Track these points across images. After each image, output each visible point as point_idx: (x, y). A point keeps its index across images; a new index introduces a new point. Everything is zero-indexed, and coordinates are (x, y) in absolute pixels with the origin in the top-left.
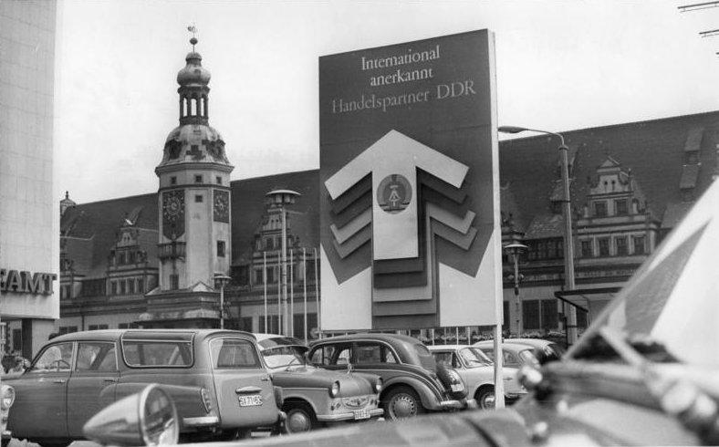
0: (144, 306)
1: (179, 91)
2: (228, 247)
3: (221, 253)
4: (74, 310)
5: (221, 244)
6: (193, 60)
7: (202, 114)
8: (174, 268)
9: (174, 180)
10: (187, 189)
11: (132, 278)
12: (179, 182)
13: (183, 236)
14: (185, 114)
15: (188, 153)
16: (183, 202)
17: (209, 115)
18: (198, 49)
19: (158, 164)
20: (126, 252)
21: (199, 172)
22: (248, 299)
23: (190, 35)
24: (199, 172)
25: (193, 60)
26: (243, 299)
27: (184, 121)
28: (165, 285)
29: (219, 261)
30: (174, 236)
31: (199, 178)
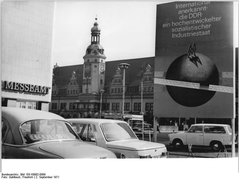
0: (77, 98)
1: (91, 34)
2: (104, 81)
3: (101, 83)
4: (57, 98)
5: (101, 80)
6: (96, 25)
7: (98, 41)
8: (87, 86)
9: (88, 60)
10: (92, 63)
11: (74, 89)
13: (91, 77)
14: (93, 41)
15: (93, 53)
16: (91, 67)
17: (100, 41)
18: (97, 21)
19: (84, 56)
20: (73, 81)
21: (96, 59)
22: (109, 97)
25: (96, 25)
26: (107, 97)
27: (92, 43)
28: (84, 92)
29: (101, 85)
30: (88, 77)
31: (96, 60)
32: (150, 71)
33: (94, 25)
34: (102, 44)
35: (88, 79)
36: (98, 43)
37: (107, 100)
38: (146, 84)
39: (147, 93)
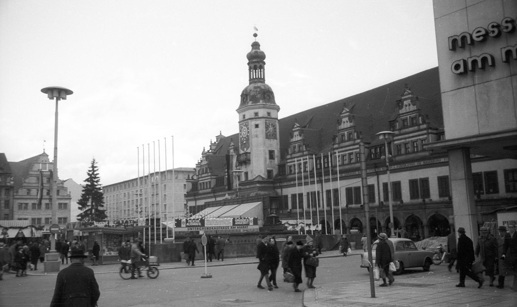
2: (277, 153)
6: (256, 45)
10: (249, 121)
12: (247, 118)
13: (249, 149)
22: (285, 184)
25: (256, 45)
27: (252, 81)
30: (245, 149)
31: (256, 114)
32: (349, 119)
33: (252, 46)
35: (246, 153)
36: (262, 80)
37: (284, 190)
38: (343, 149)
39: (347, 167)
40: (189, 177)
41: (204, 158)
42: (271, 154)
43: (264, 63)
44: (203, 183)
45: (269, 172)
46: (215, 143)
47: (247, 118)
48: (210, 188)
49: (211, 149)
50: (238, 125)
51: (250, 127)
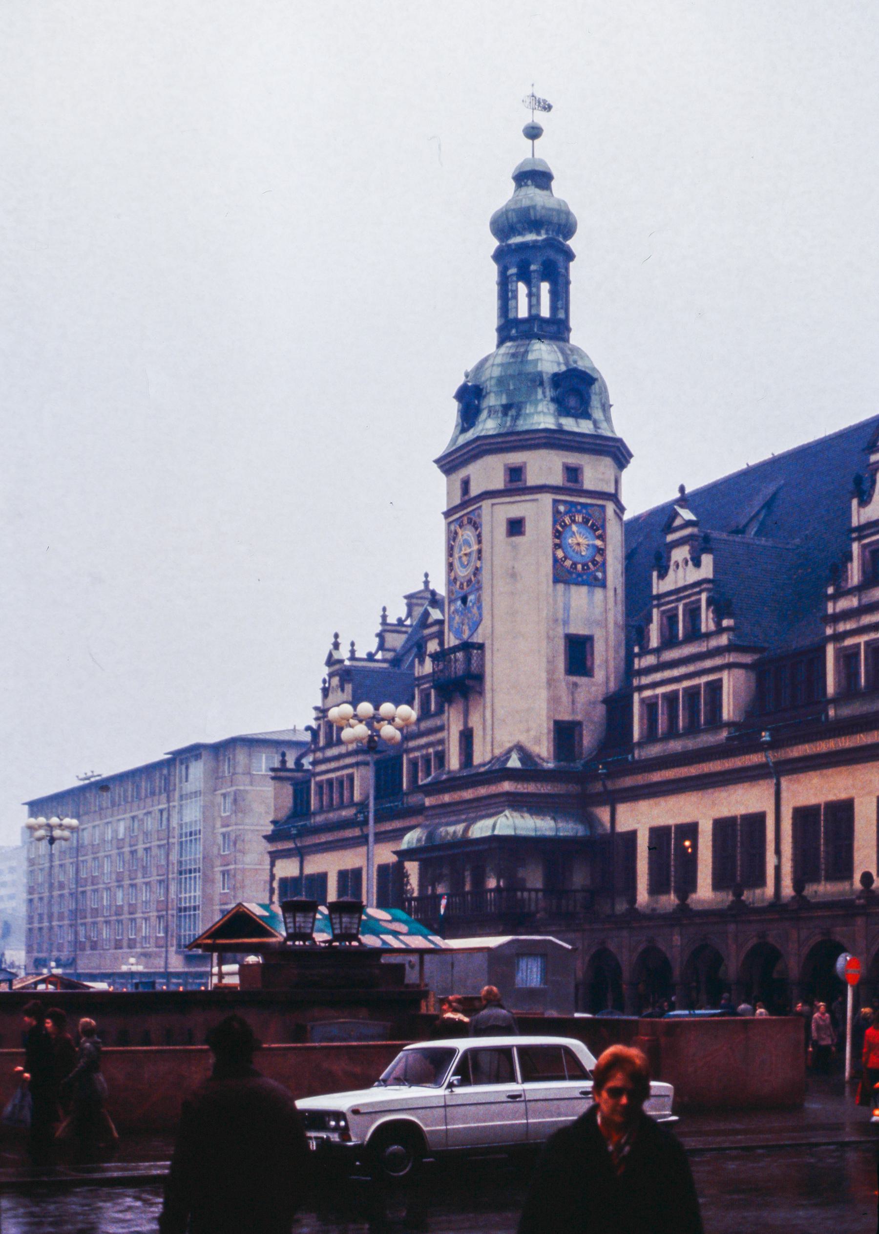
10: (486, 504)
23: (529, 116)
24: (515, 458)
31: (515, 473)
34: (594, 336)
35: (467, 647)
37: (622, 809)
40: (283, 762)
41: (336, 681)
42: (578, 653)
43: (569, 256)
44: (330, 782)
45: (565, 733)
46: (400, 622)
47: (474, 491)
48: (352, 804)
49: (381, 647)
50: (442, 523)
51: (485, 530)
